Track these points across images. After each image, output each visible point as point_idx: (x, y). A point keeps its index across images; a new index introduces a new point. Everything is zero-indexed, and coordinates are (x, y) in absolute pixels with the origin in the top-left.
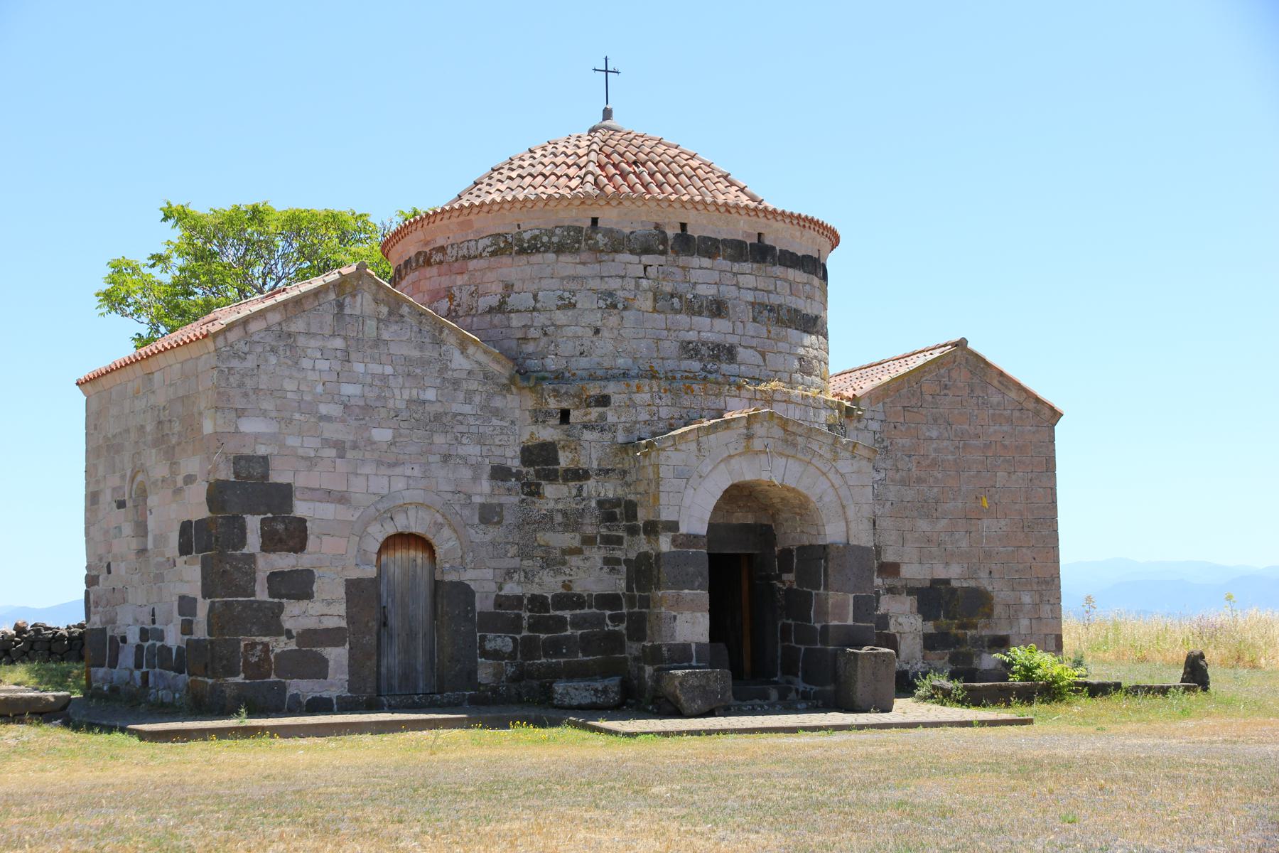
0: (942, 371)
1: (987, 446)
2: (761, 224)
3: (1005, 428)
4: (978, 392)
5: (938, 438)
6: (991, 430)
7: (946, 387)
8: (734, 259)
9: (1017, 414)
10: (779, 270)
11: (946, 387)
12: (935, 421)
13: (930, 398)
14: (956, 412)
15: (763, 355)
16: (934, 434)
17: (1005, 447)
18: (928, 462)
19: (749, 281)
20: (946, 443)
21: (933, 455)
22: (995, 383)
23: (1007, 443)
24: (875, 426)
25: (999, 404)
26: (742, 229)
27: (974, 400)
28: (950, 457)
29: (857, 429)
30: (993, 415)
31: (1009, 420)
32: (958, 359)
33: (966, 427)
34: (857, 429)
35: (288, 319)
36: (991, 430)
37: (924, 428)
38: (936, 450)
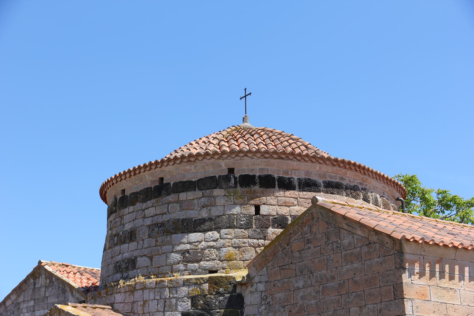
0: (305, 229)
1: (341, 285)
2: (158, 173)
3: (355, 265)
4: (333, 238)
5: (304, 287)
6: (344, 269)
7: (309, 241)
8: (144, 201)
9: (365, 249)
10: (171, 198)
11: (309, 241)
12: (301, 272)
13: (297, 254)
14: (316, 260)
15: (151, 258)
16: (301, 284)
17: (356, 283)
18: (297, 309)
19: (151, 211)
20: (309, 290)
21: (300, 302)
22: (345, 227)
23: (357, 279)
24: (261, 287)
25: (350, 244)
26: (149, 180)
27: (330, 247)
28: (313, 302)
29: (251, 292)
30: (346, 256)
31: (358, 257)
32: (315, 214)
33: (324, 272)
34: (251, 292)
35: (18, 296)
36: (344, 269)
37: (293, 280)
38: (303, 298)
